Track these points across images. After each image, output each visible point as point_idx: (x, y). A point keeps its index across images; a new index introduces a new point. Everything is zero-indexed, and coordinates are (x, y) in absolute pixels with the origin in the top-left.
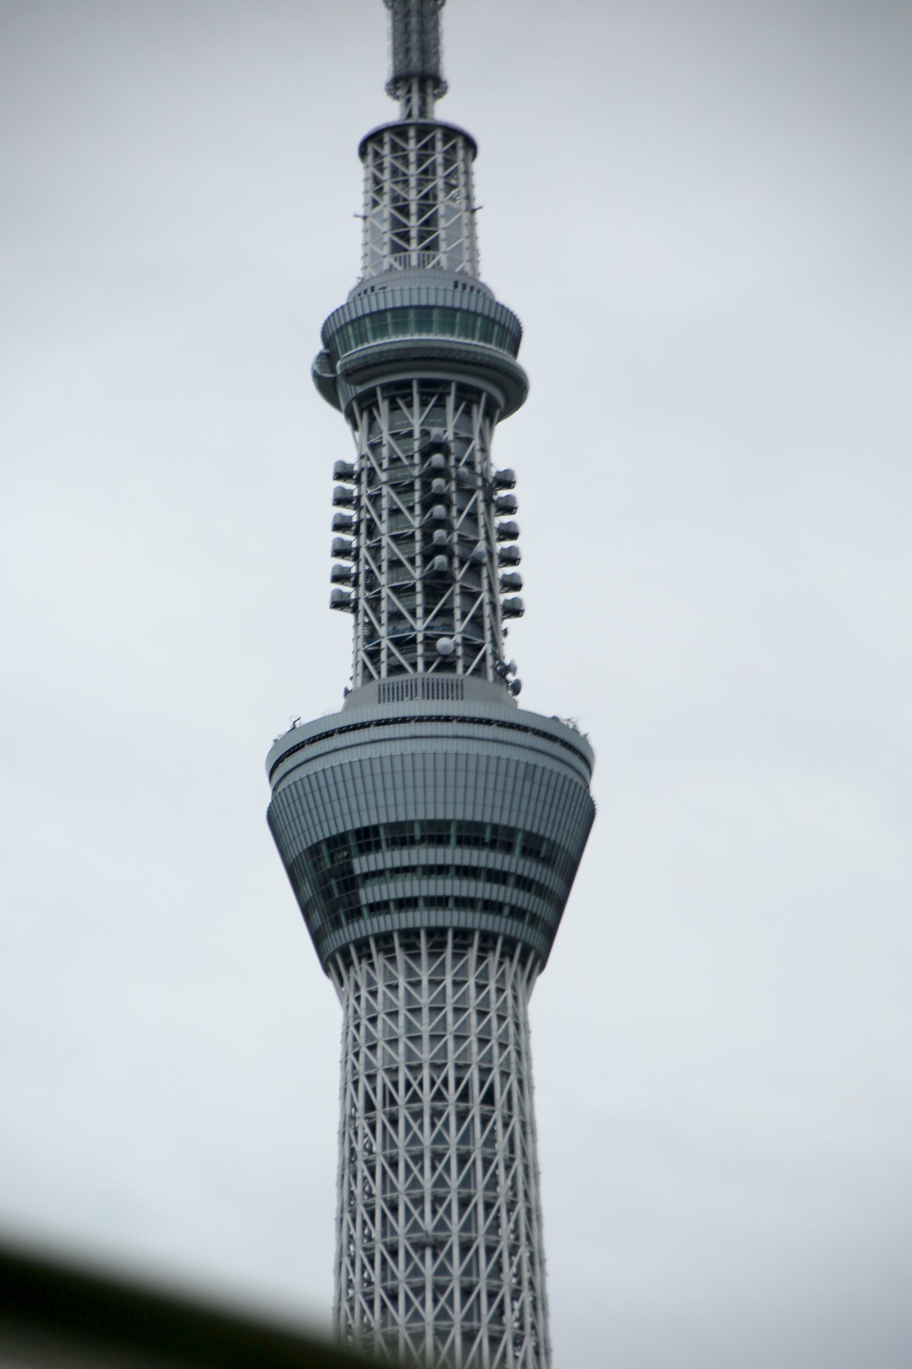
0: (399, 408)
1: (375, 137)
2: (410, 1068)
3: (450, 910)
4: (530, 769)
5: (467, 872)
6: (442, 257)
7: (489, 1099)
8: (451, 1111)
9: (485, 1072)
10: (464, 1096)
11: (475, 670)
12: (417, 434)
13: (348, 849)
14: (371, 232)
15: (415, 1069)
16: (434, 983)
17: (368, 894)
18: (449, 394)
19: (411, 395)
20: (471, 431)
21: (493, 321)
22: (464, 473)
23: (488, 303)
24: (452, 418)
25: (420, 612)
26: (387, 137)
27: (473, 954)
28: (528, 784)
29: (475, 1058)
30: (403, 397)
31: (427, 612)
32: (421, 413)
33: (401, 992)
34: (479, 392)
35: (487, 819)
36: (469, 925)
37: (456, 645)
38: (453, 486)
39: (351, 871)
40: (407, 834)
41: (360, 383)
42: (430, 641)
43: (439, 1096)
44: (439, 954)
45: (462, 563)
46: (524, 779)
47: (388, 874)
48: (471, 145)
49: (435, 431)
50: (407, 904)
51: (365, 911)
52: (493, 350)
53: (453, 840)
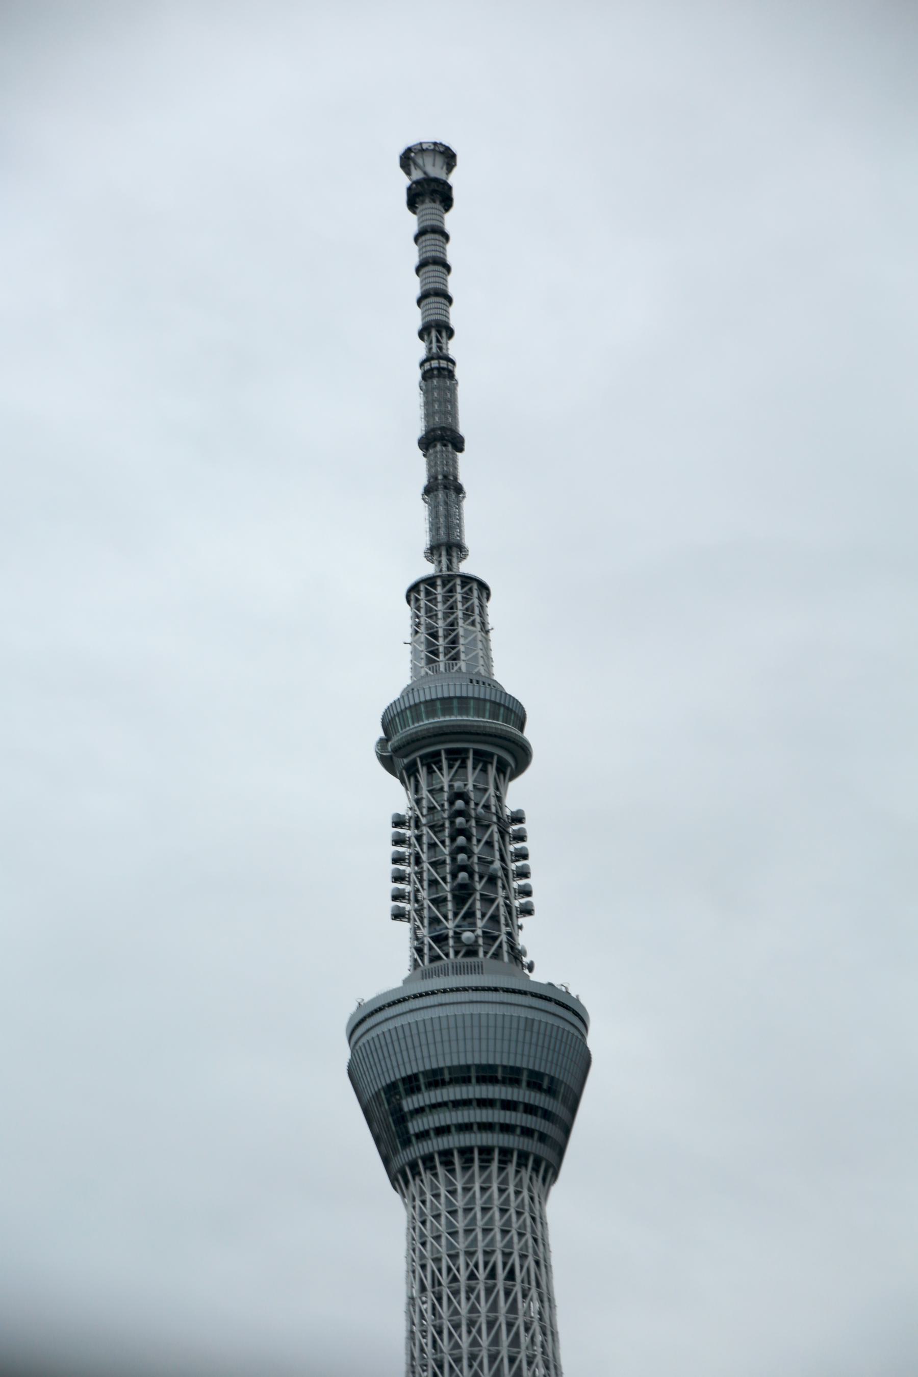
0: (434, 772)
1: (414, 588)
2: (450, 1256)
3: (475, 1133)
4: (529, 1022)
5: (484, 1103)
6: (462, 665)
7: (511, 1276)
8: (481, 1287)
9: (507, 1255)
10: (492, 1275)
11: (493, 954)
12: (446, 788)
13: (399, 1093)
14: (415, 652)
15: (454, 1257)
16: (466, 1190)
17: (415, 1126)
18: (468, 758)
19: (440, 761)
20: (487, 783)
21: (499, 704)
22: (481, 813)
23: (499, 693)
24: (471, 776)
25: (450, 915)
26: (422, 587)
27: (495, 1165)
28: (528, 1034)
29: (499, 1244)
30: (435, 763)
31: (456, 915)
32: (449, 773)
33: (443, 1199)
34: (491, 755)
35: (498, 1062)
36: (490, 1143)
37: (477, 937)
38: (473, 823)
39: (401, 1109)
40: (439, 1078)
41: (406, 756)
42: (457, 936)
43: (472, 1276)
44: (469, 1168)
45: (481, 878)
46: (525, 1030)
47: (427, 1110)
48: (484, 588)
49: (457, 784)
50: (442, 1131)
51: (414, 1139)
52: (500, 725)
53: (474, 1080)
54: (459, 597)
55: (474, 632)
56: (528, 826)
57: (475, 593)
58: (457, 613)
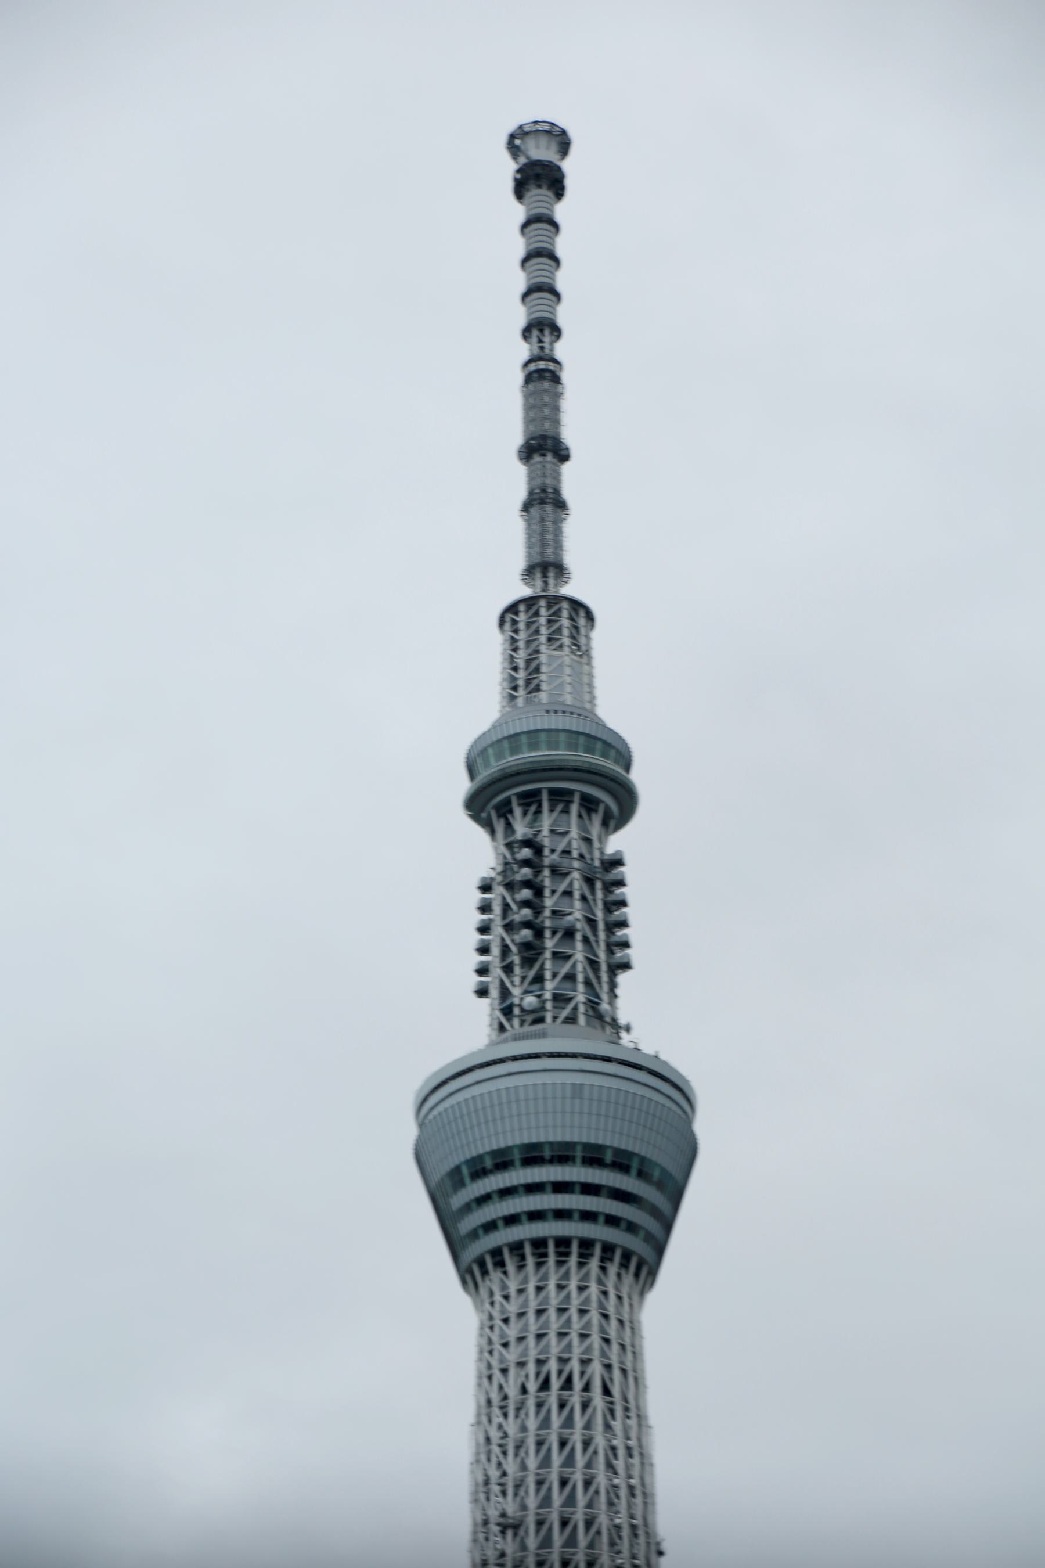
6: (543, 696)
7: (568, 1385)
10: (545, 1385)
11: (567, 1018)
34: (571, 792)
38: (546, 872)
54: (543, 620)
55: (561, 657)
56: (627, 871)
57: (565, 614)
58: (563, 641)
